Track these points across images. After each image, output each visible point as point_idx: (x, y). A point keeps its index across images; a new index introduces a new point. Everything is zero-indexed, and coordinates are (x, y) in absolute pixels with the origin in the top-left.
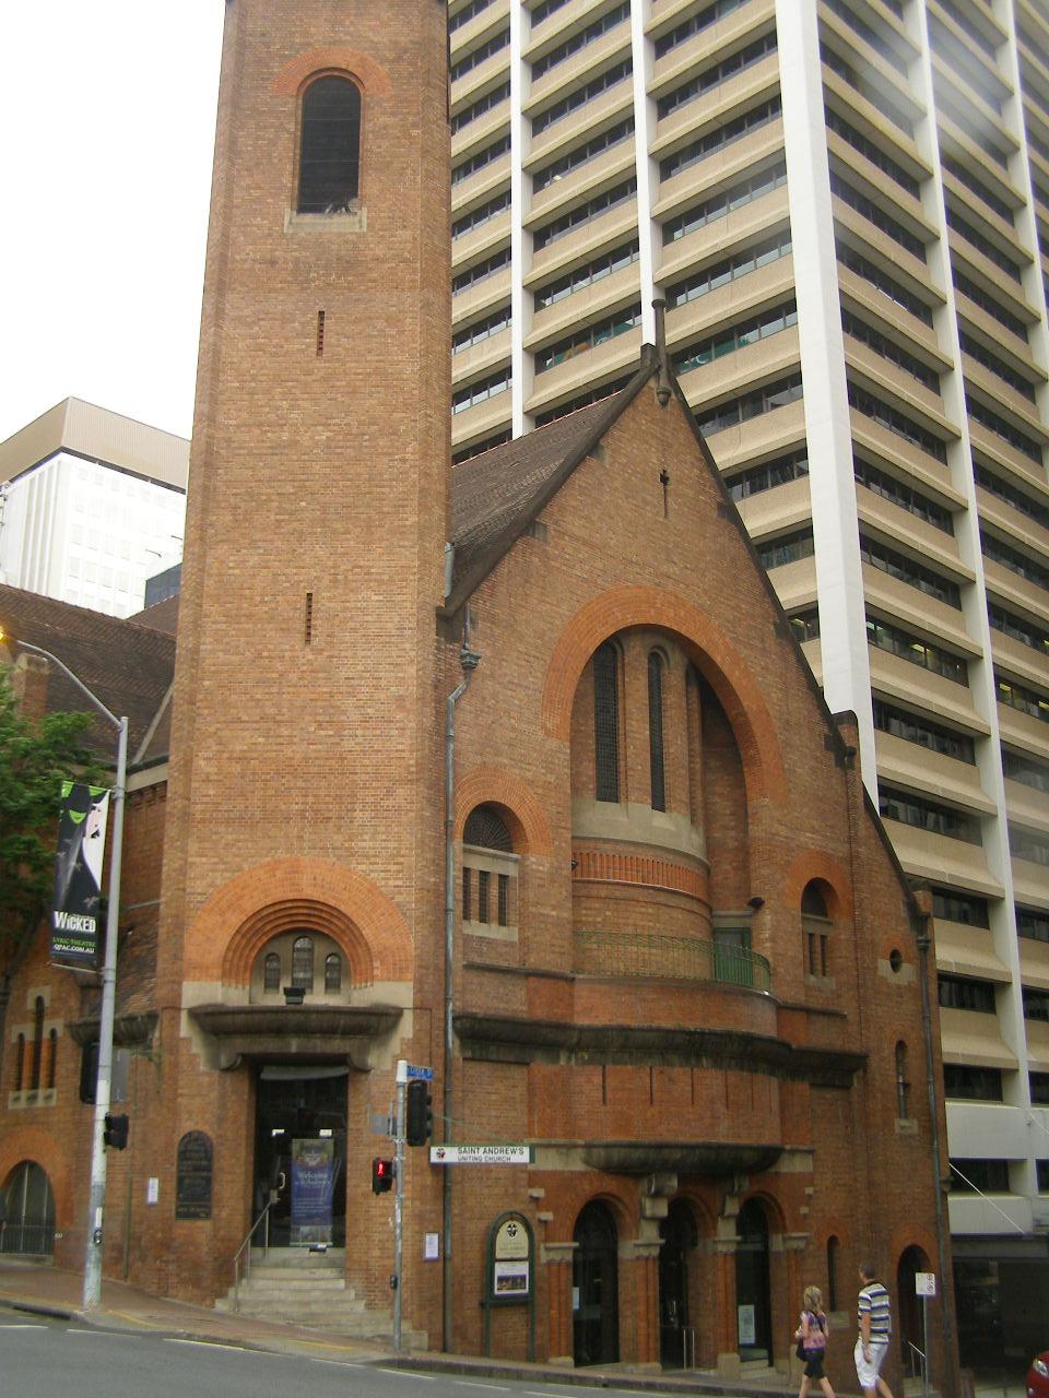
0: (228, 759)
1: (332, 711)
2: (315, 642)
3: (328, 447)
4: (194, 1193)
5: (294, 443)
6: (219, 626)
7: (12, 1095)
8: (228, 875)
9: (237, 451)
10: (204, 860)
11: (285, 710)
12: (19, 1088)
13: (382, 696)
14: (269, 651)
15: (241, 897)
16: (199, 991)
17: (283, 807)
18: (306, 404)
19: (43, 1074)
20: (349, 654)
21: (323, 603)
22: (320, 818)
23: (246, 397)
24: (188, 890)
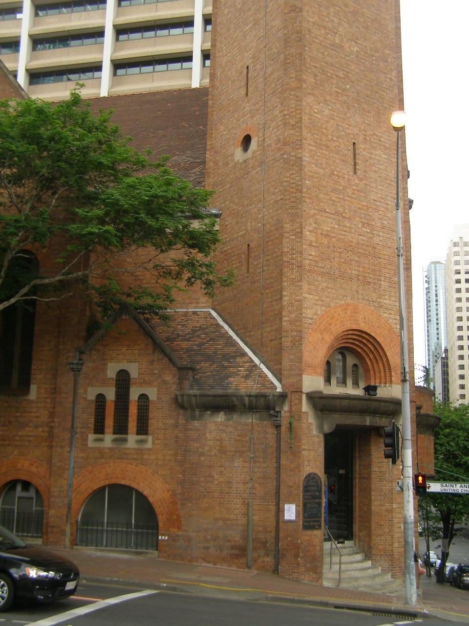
0: (321, 234)
1: (369, 217)
2: (358, 173)
3: (357, 56)
6: (312, 148)
7: (91, 437)
8: (323, 308)
9: (314, 39)
10: (311, 296)
11: (347, 211)
12: (99, 429)
13: (390, 215)
14: (337, 171)
15: (330, 324)
16: (312, 382)
17: (349, 271)
18: (346, 25)
19: (132, 425)
20: (374, 185)
23: (317, 6)
24: (304, 315)
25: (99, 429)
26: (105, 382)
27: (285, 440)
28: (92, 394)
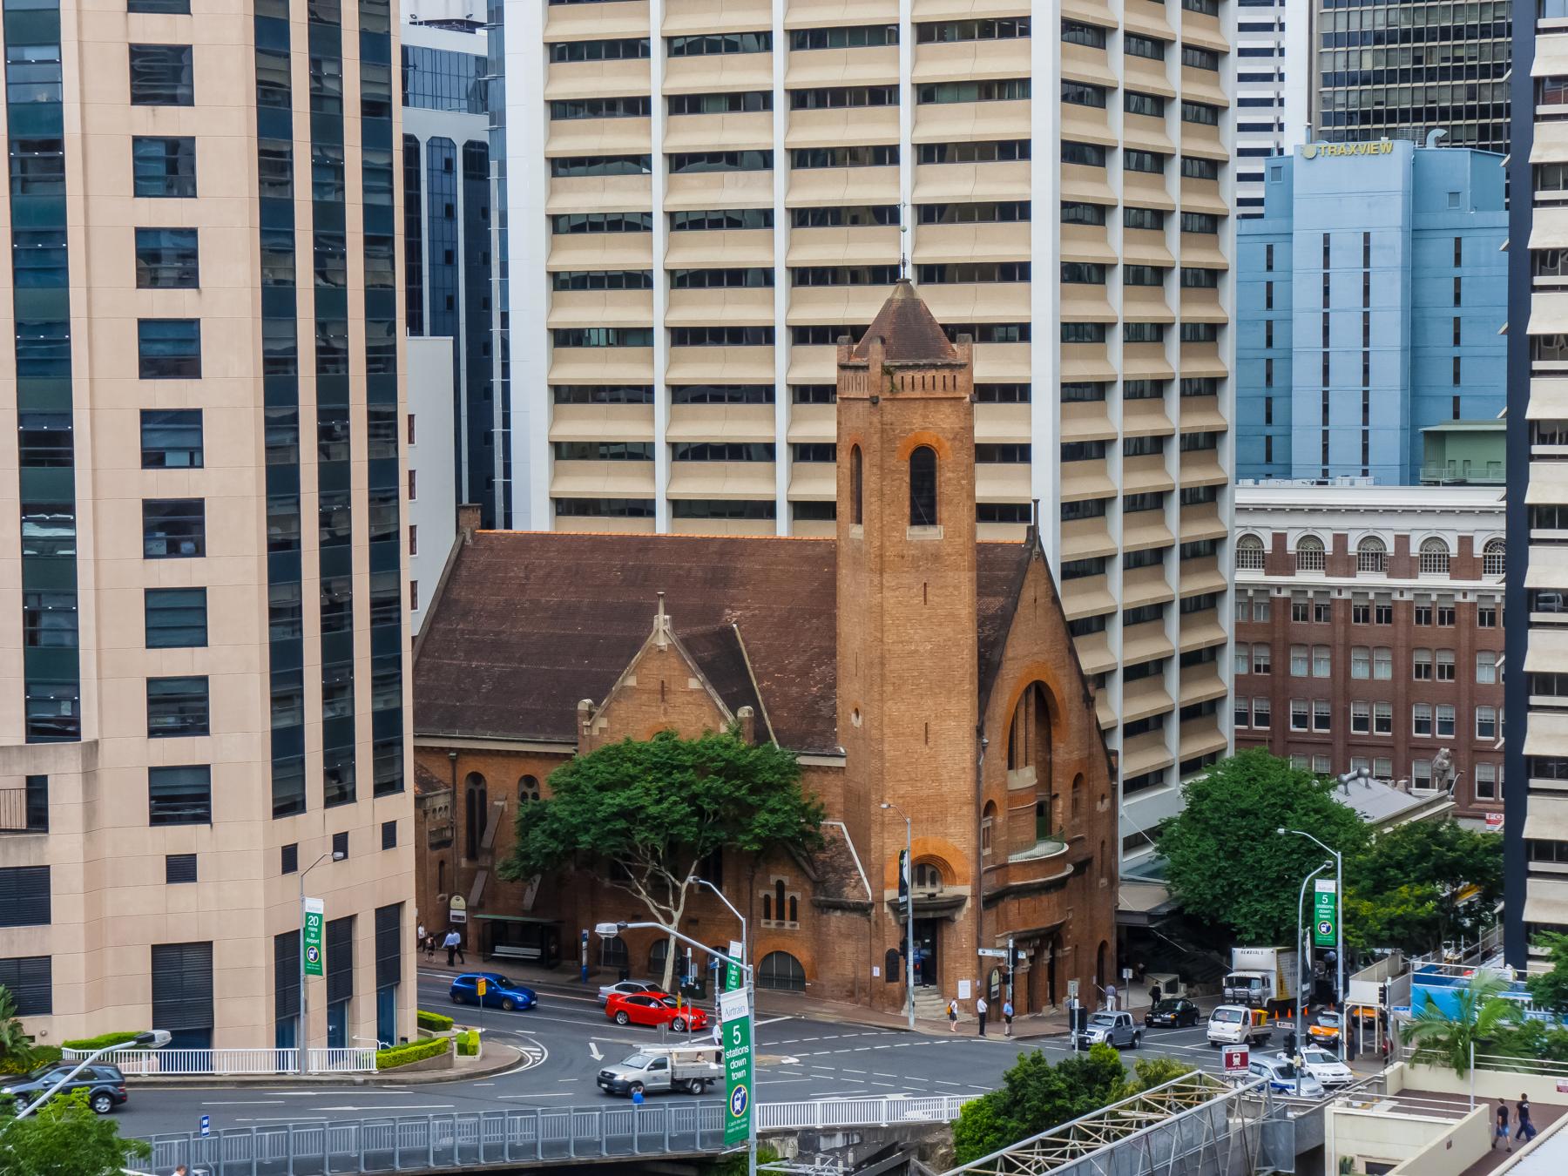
4: (892, 972)
5: (916, 651)
12: (768, 916)
19: (787, 914)
21: (933, 727)
22: (933, 820)
25: (768, 916)
26: (769, 887)
27: (878, 930)
28: (762, 893)
